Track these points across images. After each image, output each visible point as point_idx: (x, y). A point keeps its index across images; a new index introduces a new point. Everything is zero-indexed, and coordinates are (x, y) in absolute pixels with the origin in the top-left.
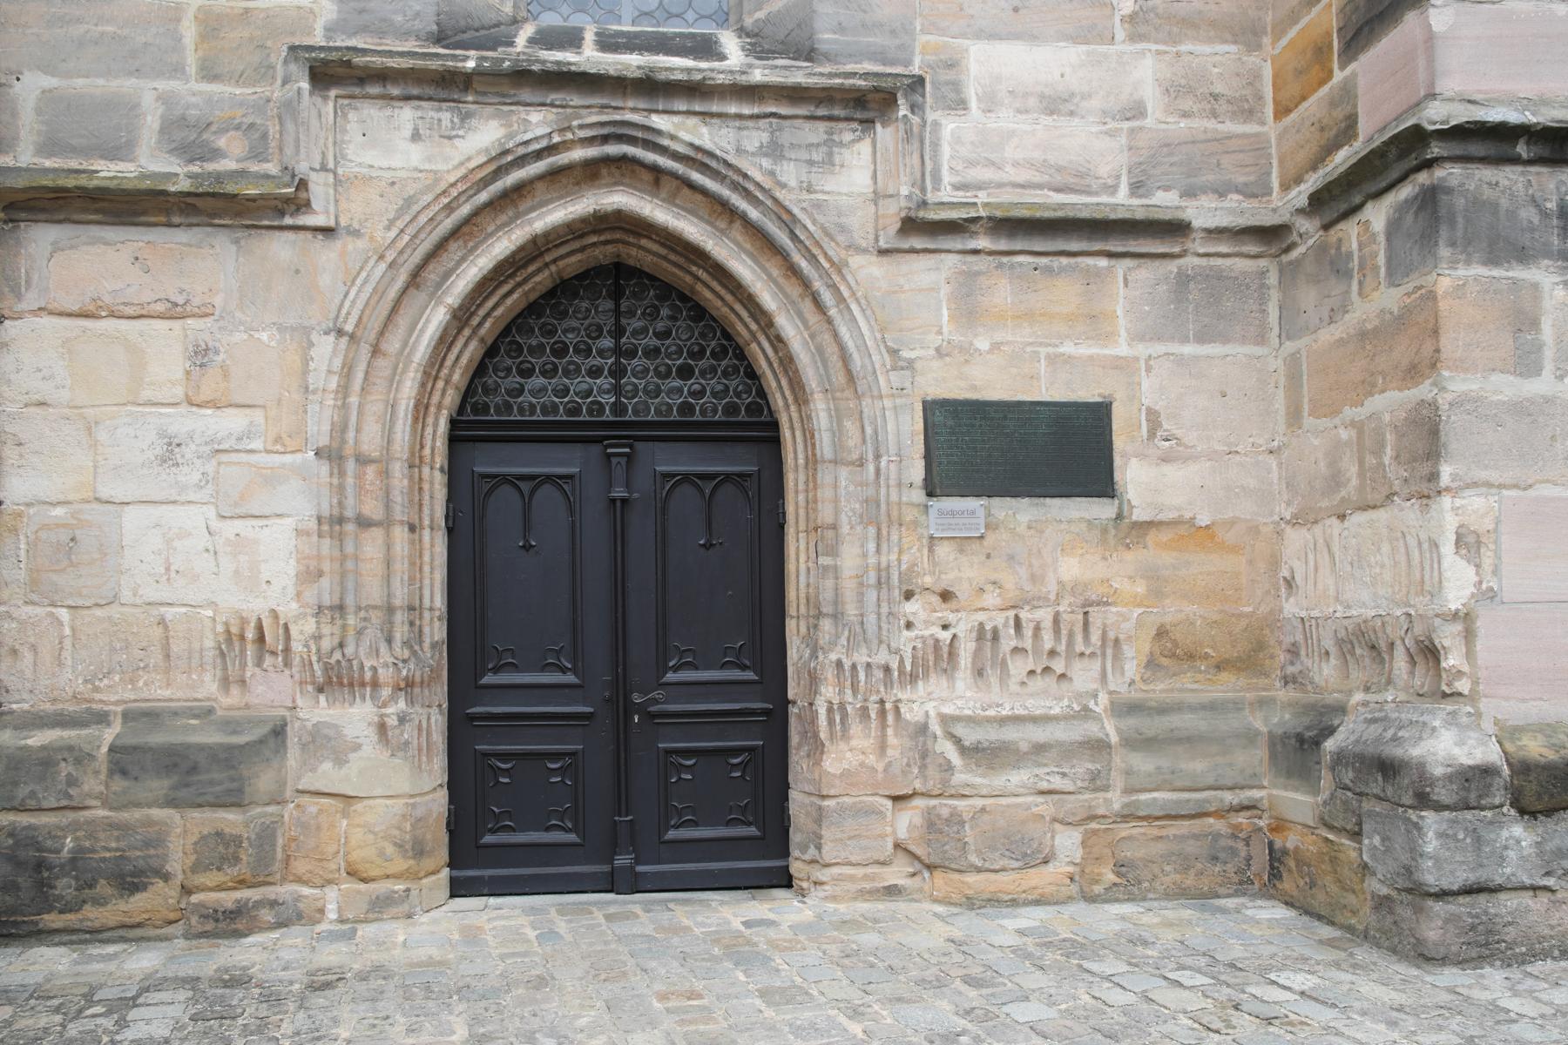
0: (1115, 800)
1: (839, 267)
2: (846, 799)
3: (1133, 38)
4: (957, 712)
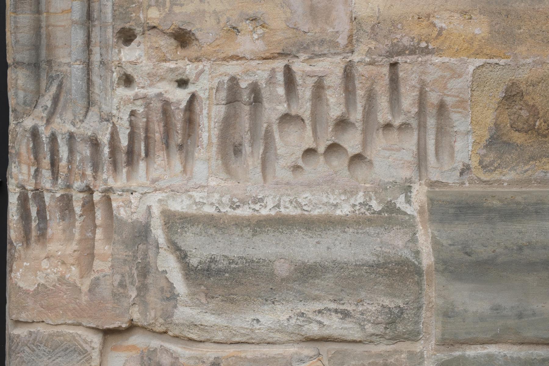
2: (40, 328)
4: (194, 210)
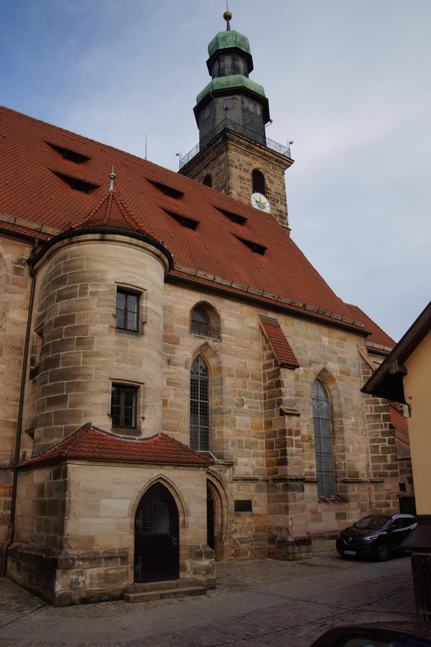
0: (254, 547)
1: (227, 484)
3: (253, 457)
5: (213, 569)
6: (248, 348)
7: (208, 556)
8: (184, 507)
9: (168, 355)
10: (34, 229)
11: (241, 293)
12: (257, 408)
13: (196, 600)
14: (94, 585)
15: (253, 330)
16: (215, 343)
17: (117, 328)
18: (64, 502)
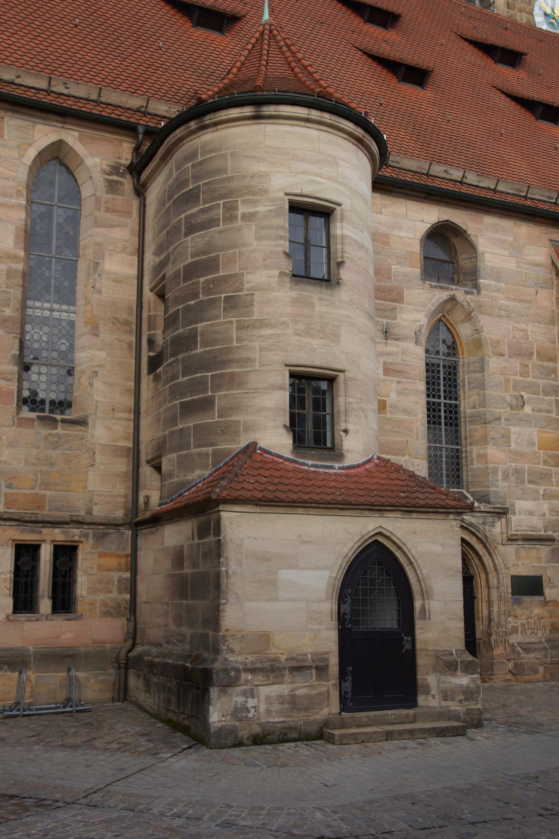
0: (549, 660)
1: (496, 547)
3: (544, 499)
5: (476, 692)
6: (530, 302)
7: (468, 668)
8: (423, 584)
9: (385, 321)
10: (135, 108)
11: (516, 200)
12: (549, 411)
13: (449, 744)
14: (274, 713)
15: (539, 269)
16: (469, 297)
17: (294, 276)
18: (218, 575)
